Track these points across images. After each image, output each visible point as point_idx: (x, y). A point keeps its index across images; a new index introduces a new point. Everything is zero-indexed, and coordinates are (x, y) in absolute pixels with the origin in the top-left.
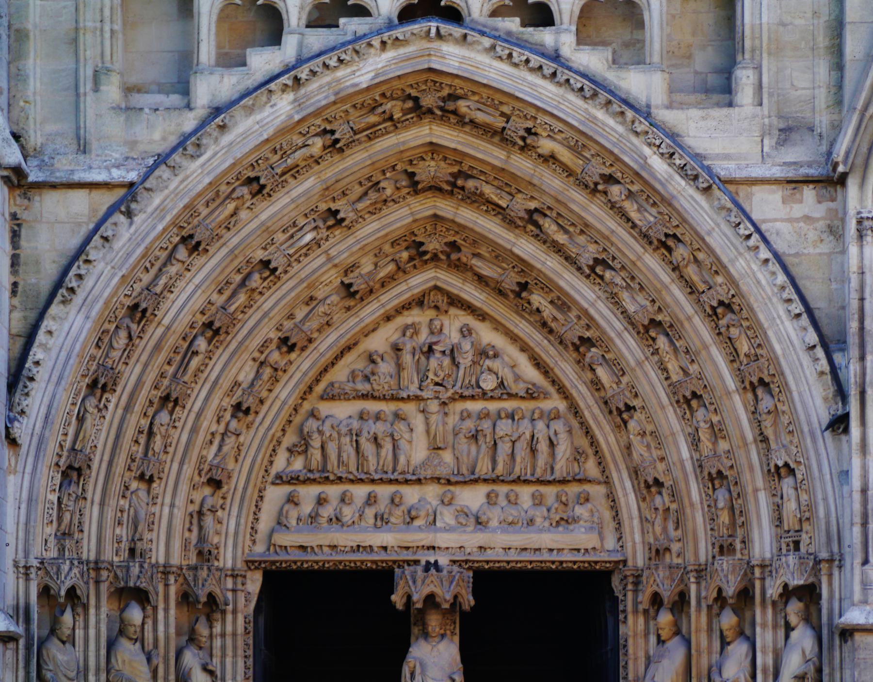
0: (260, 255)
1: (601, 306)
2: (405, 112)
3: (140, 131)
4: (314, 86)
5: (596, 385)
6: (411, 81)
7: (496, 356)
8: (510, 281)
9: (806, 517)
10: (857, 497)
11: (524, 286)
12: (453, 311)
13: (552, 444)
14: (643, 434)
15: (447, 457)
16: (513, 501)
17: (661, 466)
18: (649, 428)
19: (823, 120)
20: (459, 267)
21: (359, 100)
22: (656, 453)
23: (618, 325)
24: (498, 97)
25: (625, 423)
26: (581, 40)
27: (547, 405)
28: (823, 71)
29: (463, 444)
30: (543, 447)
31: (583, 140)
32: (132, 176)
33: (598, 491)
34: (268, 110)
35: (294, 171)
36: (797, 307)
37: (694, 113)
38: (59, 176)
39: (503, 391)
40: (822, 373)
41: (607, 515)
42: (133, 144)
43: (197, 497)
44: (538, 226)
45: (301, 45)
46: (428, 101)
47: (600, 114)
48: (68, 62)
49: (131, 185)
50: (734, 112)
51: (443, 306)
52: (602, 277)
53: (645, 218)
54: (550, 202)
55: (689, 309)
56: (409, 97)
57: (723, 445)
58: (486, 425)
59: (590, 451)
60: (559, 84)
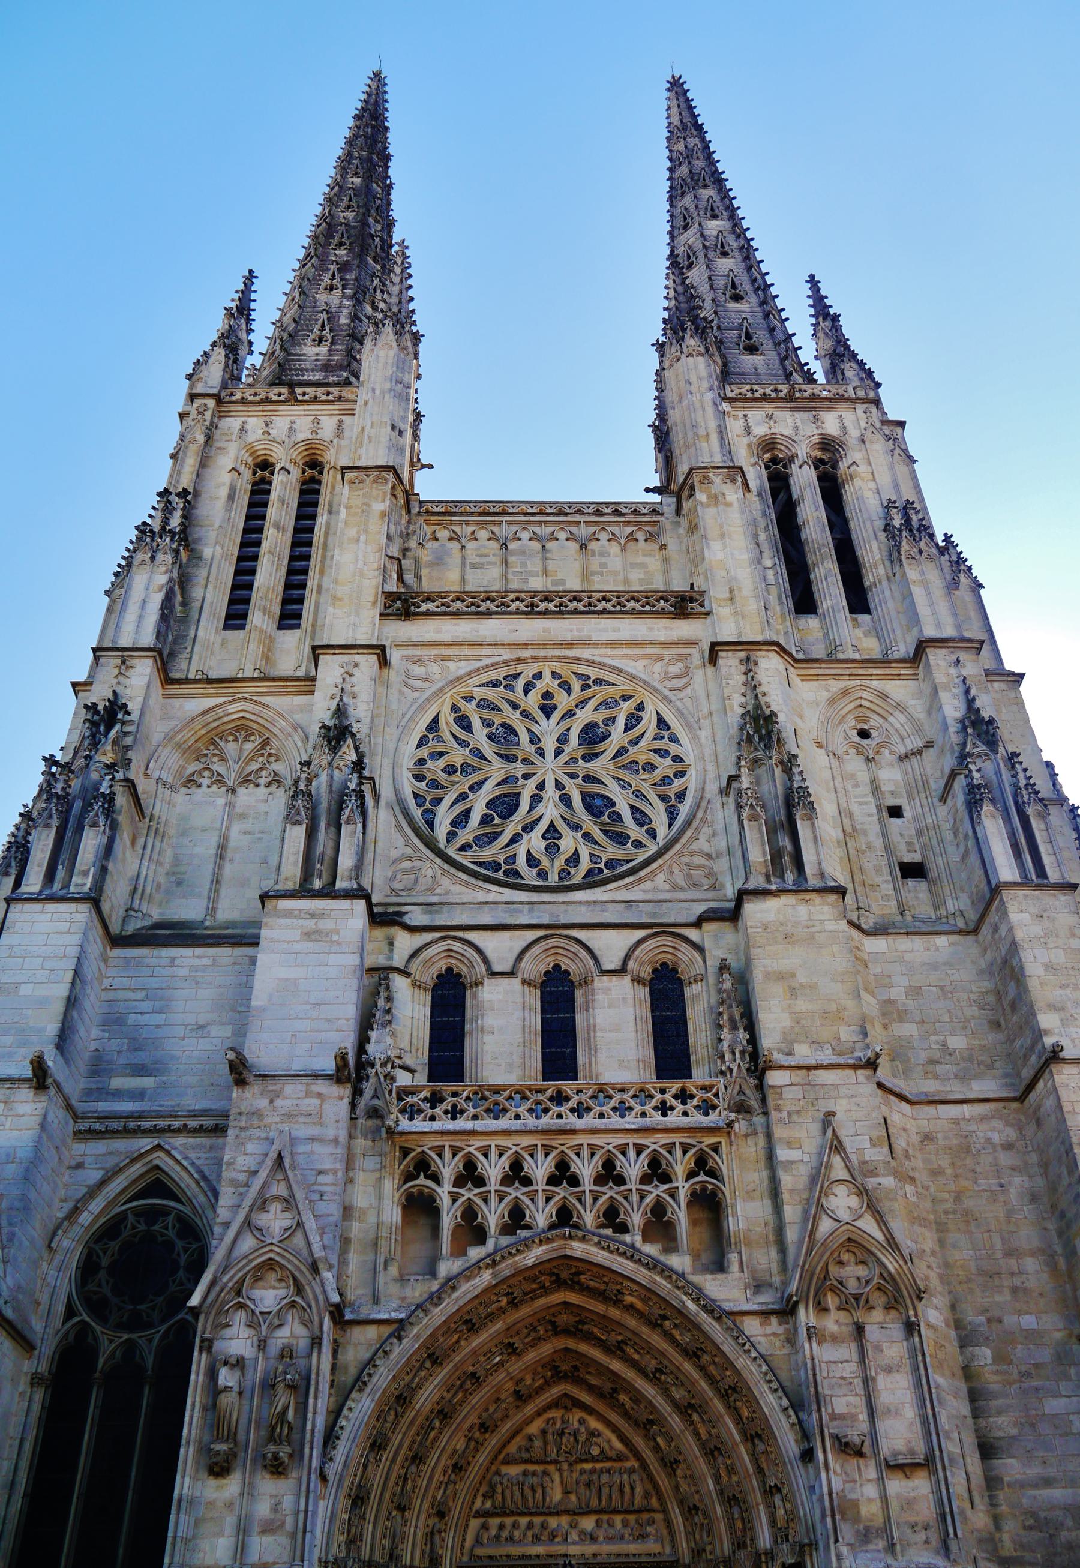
0: (471, 1369)
1: (659, 1398)
2: (552, 1282)
3: (408, 1292)
4: (503, 1265)
5: (657, 1449)
6: (555, 1263)
7: (599, 1435)
8: (608, 1386)
9: (792, 1517)
10: (826, 1498)
11: (615, 1390)
12: (575, 1410)
13: (632, 1488)
14: (685, 1477)
15: (573, 1498)
16: (611, 1524)
17: (697, 1497)
18: (688, 1473)
19: (777, 1280)
20: (579, 1382)
21: (527, 1274)
22: (693, 1489)
23: (668, 1409)
24: (602, 1272)
25: (674, 1471)
26: (645, 1240)
27: (628, 1464)
28: (774, 1253)
29: (582, 1489)
30: (627, 1489)
31: (648, 1295)
32: (402, 1316)
33: (659, 1517)
34: (478, 1279)
35: (491, 1317)
36: (775, 1385)
37: (709, 1277)
38: (362, 1316)
39: (604, 1457)
40: (793, 1424)
41: (665, 1532)
42: (403, 1299)
43: (431, 1522)
44: (623, 1351)
45: (496, 1244)
46: (564, 1275)
47: (658, 1278)
48: (371, 1256)
49: (402, 1320)
50: (730, 1276)
51: (569, 1405)
52: (659, 1380)
53: (684, 1338)
54: (629, 1335)
55: (711, 1394)
56: (554, 1274)
57: (735, 1479)
58: (595, 1477)
59: (653, 1492)
60: (635, 1262)
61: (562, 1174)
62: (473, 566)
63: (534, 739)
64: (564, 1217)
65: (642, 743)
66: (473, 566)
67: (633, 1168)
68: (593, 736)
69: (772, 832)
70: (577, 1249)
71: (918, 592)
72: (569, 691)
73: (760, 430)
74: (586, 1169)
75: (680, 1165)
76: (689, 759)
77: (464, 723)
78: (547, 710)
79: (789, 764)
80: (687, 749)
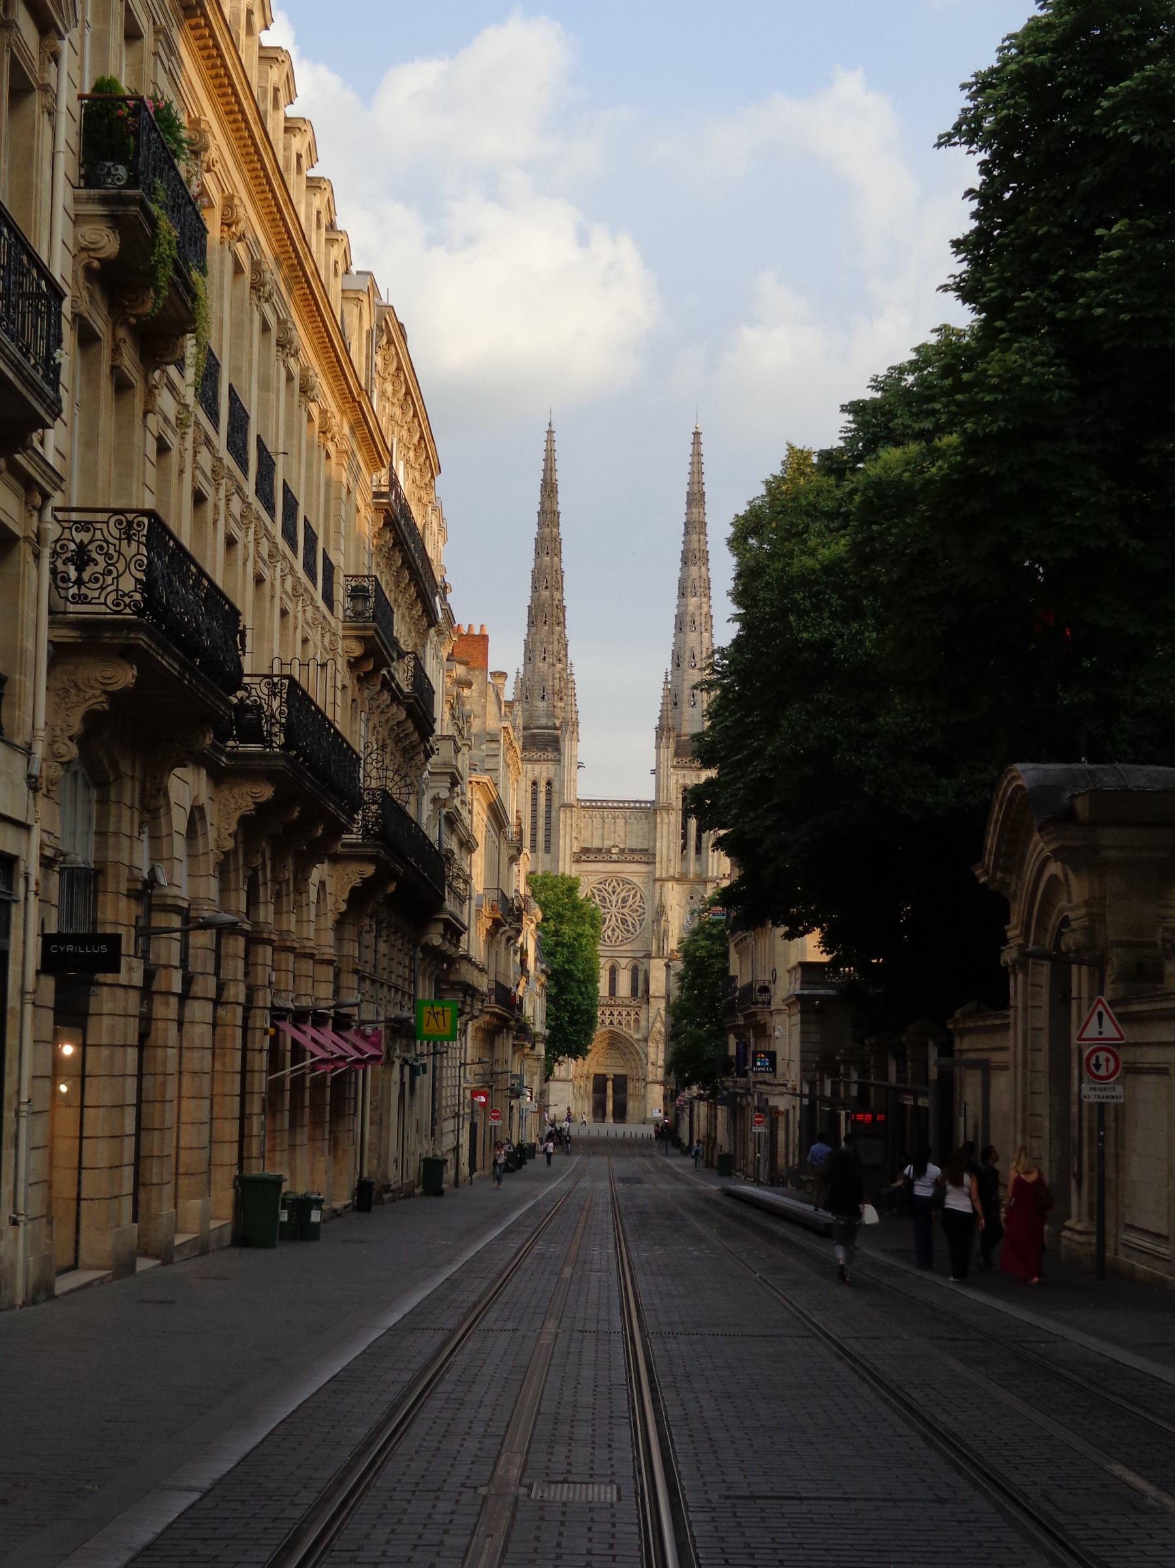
61: (611, 1014)
62: (596, 829)
63: (610, 902)
64: (611, 1023)
65: (637, 904)
66: (596, 829)
67: (624, 1013)
68: (624, 901)
69: (659, 940)
70: (613, 1029)
71: (710, 859)
72: (619, 885)
73: (681, 781)
74: (616, 1013)
75: (633, 1013)
76: (646, 911)
77: (594, 894)
78: (614, 892)
79: (667, 921)
80: (645, 907)
